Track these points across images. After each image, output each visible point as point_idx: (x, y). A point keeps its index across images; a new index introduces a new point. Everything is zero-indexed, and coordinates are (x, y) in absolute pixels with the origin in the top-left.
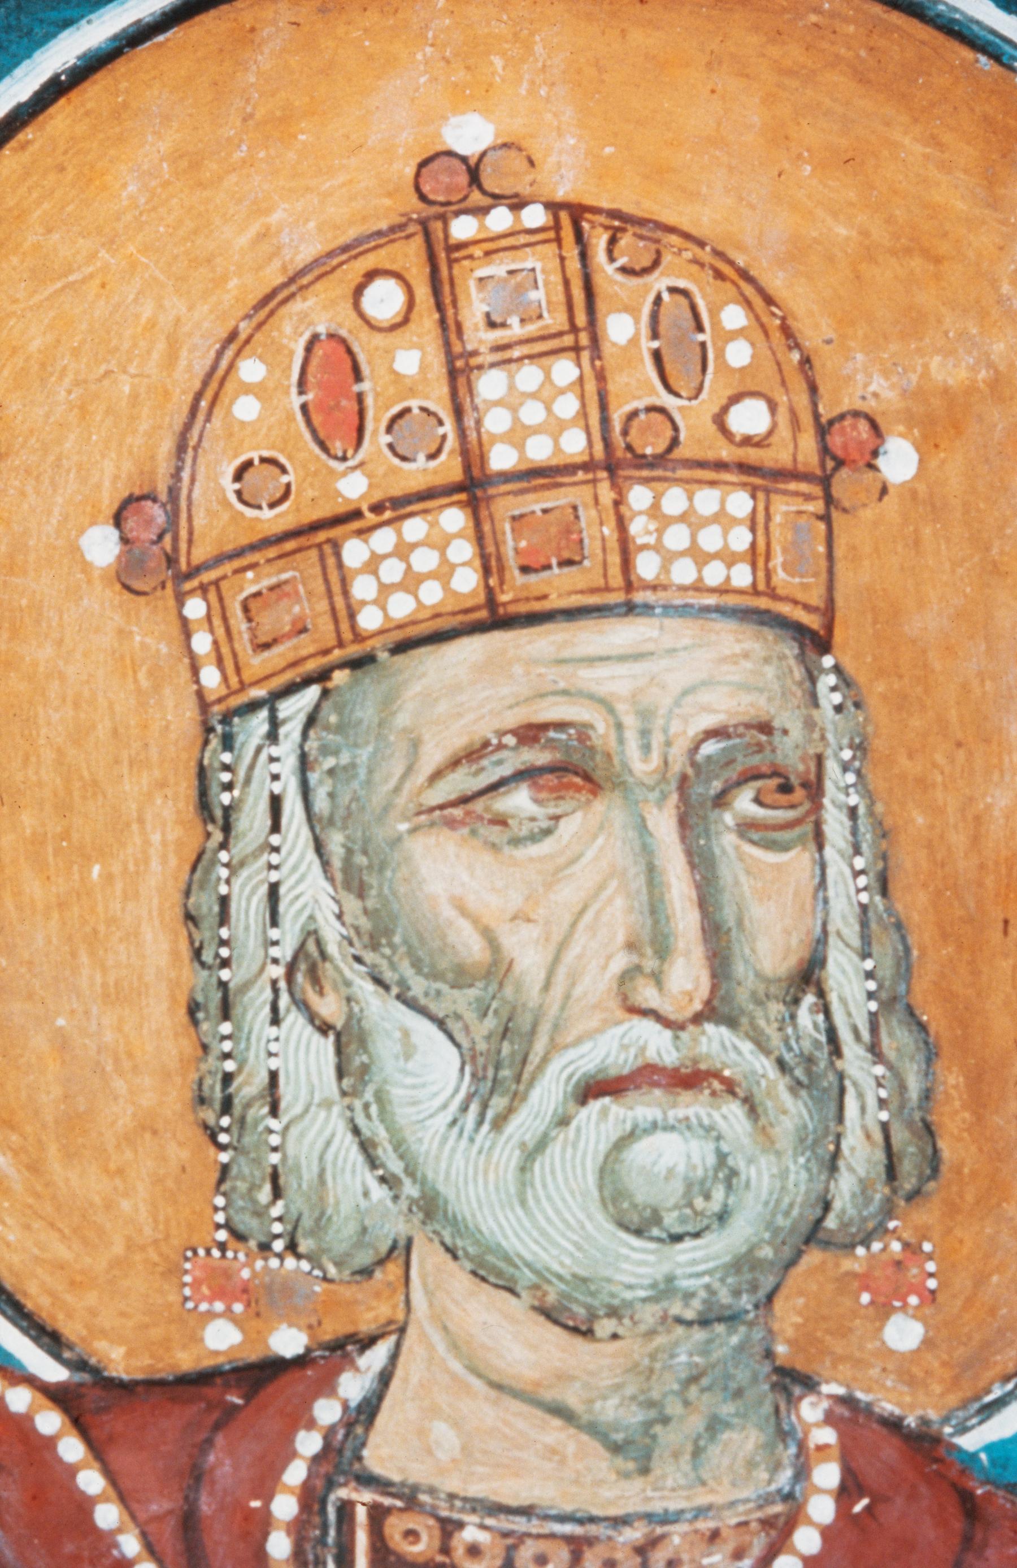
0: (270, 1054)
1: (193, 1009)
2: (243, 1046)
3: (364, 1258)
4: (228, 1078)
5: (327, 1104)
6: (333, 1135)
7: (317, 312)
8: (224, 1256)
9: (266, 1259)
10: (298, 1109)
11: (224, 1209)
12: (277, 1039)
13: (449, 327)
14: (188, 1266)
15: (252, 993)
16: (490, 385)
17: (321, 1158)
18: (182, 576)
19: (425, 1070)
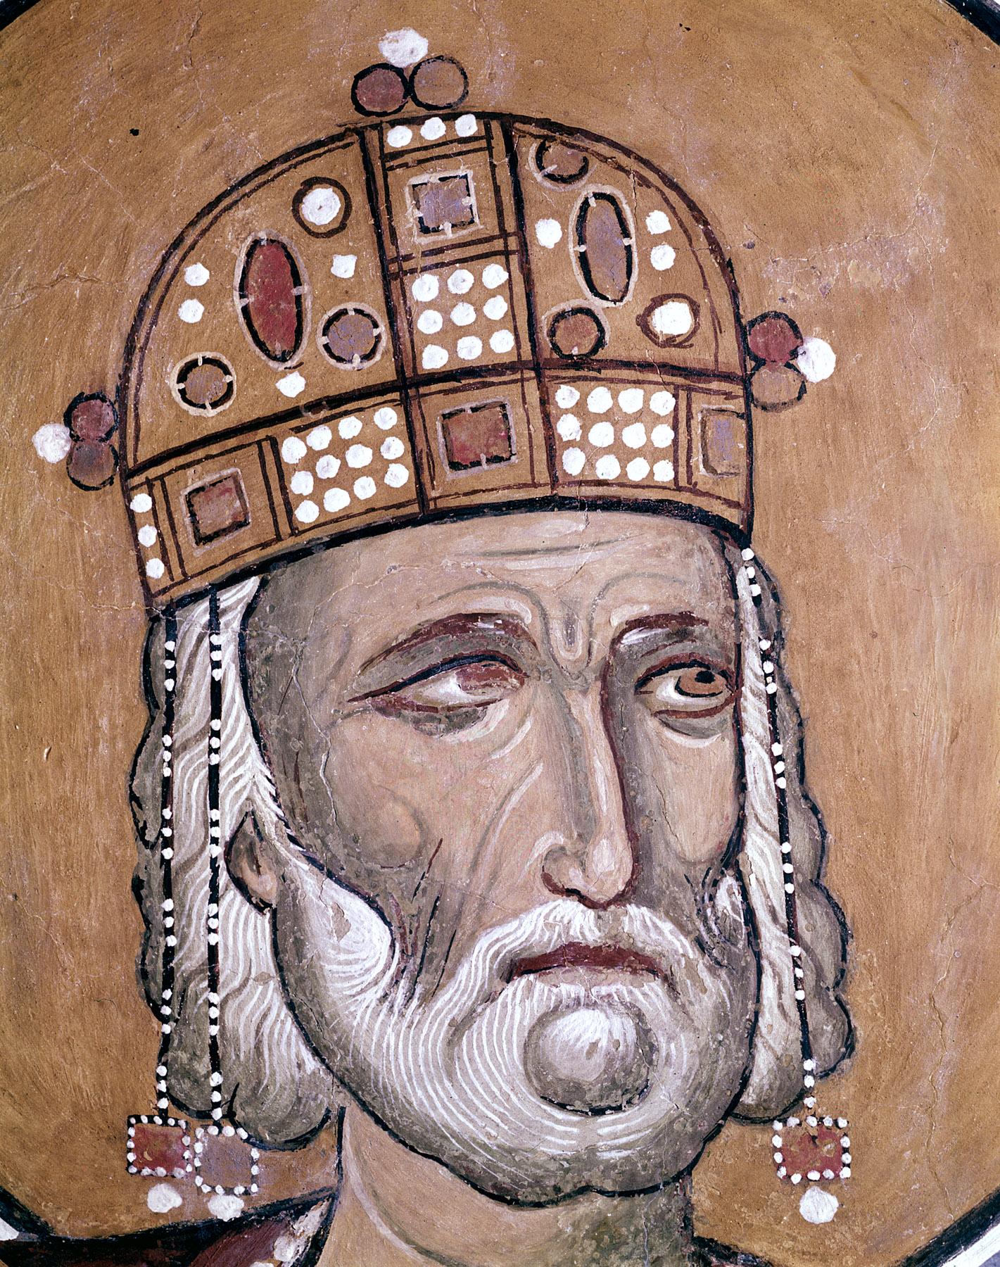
0: (210, 930)
1: (137, 885)
2: (183, 922)
3: (298, 1128)
4: (170, 953)
5: (263, 979)
6: (269, 1009)
7: (259, 217)
8: (165, 1123)
9: (205, 1127)
10: (236, 983)
11: (165, 1078)
12: (216, 916)
13: (383, 234)
14: (132, 1132)
15: (195, 870)
16: (424, 288)
17: (257, 1032)
18: (128, 474)
19: (353, 948)
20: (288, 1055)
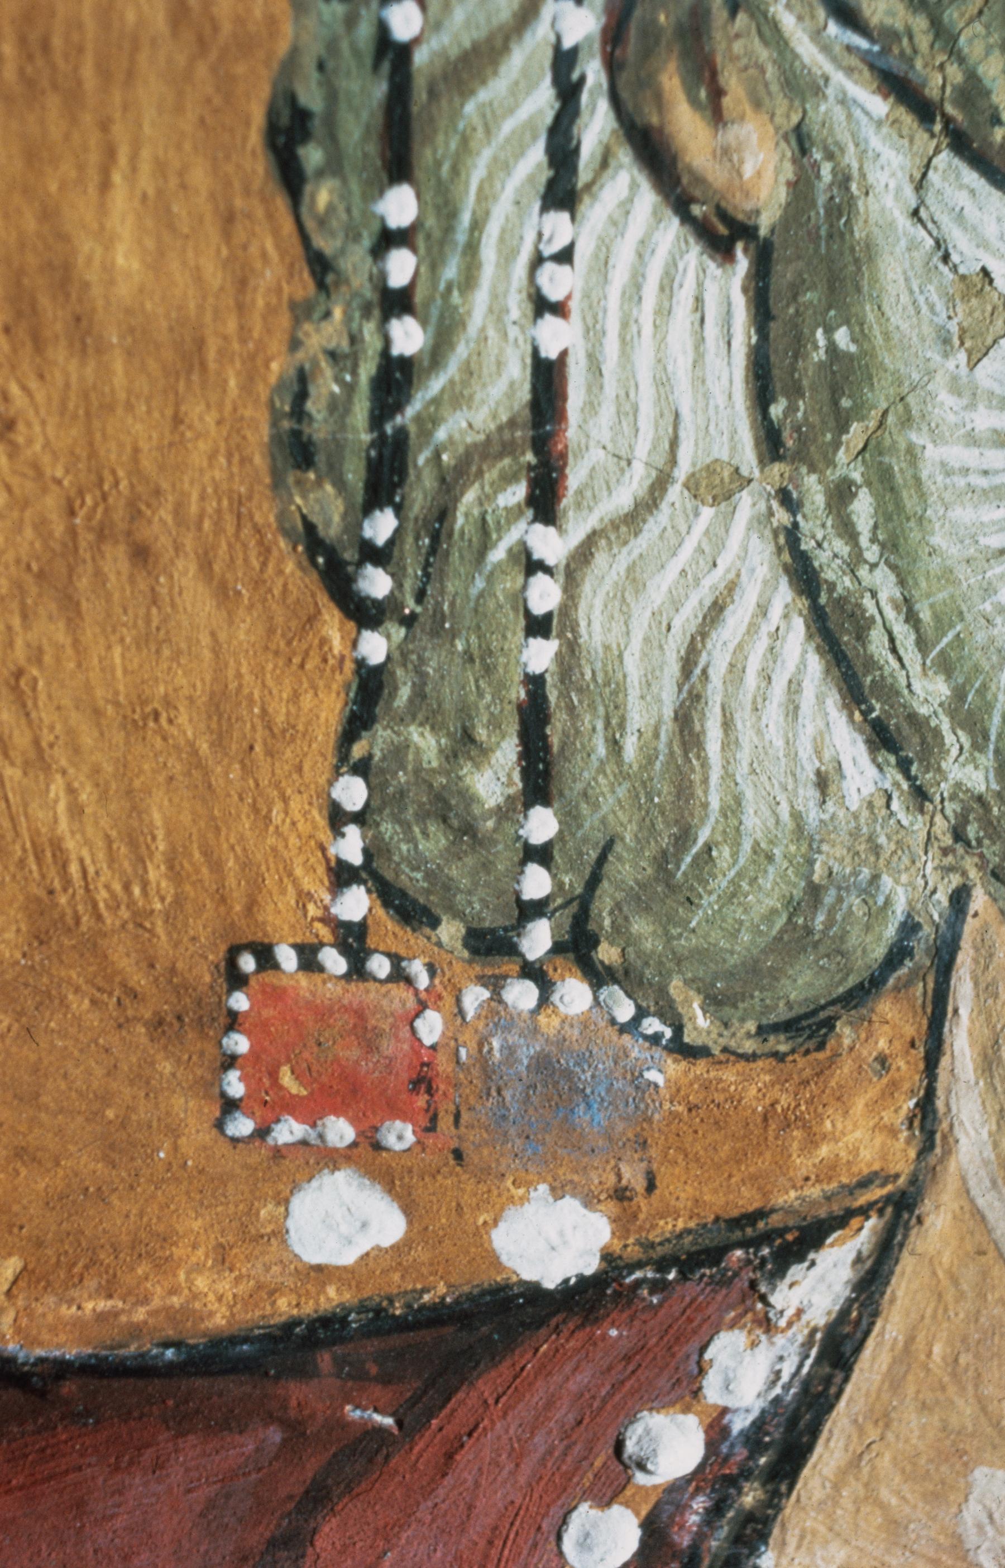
0: (542, 306)
1: (288, 133)
2: (451, 271)
3: (803, 984)
4: (395, 378)
5: (717, 487)
6: (732, 587)
8: (358, 971)
9: (495, 984)
10: (622, 499)
11: (359, 818)
12: (565, 256)
14: (240, 1002)
15: (494, 89)
17: (688, 663)
20: (785, 748)
